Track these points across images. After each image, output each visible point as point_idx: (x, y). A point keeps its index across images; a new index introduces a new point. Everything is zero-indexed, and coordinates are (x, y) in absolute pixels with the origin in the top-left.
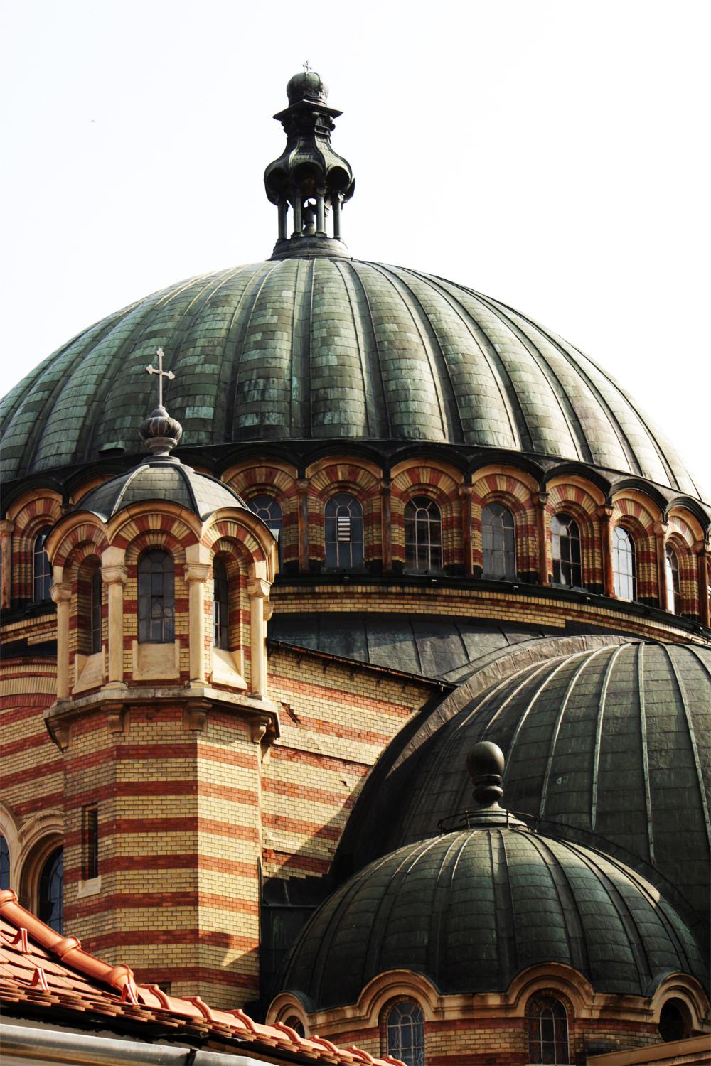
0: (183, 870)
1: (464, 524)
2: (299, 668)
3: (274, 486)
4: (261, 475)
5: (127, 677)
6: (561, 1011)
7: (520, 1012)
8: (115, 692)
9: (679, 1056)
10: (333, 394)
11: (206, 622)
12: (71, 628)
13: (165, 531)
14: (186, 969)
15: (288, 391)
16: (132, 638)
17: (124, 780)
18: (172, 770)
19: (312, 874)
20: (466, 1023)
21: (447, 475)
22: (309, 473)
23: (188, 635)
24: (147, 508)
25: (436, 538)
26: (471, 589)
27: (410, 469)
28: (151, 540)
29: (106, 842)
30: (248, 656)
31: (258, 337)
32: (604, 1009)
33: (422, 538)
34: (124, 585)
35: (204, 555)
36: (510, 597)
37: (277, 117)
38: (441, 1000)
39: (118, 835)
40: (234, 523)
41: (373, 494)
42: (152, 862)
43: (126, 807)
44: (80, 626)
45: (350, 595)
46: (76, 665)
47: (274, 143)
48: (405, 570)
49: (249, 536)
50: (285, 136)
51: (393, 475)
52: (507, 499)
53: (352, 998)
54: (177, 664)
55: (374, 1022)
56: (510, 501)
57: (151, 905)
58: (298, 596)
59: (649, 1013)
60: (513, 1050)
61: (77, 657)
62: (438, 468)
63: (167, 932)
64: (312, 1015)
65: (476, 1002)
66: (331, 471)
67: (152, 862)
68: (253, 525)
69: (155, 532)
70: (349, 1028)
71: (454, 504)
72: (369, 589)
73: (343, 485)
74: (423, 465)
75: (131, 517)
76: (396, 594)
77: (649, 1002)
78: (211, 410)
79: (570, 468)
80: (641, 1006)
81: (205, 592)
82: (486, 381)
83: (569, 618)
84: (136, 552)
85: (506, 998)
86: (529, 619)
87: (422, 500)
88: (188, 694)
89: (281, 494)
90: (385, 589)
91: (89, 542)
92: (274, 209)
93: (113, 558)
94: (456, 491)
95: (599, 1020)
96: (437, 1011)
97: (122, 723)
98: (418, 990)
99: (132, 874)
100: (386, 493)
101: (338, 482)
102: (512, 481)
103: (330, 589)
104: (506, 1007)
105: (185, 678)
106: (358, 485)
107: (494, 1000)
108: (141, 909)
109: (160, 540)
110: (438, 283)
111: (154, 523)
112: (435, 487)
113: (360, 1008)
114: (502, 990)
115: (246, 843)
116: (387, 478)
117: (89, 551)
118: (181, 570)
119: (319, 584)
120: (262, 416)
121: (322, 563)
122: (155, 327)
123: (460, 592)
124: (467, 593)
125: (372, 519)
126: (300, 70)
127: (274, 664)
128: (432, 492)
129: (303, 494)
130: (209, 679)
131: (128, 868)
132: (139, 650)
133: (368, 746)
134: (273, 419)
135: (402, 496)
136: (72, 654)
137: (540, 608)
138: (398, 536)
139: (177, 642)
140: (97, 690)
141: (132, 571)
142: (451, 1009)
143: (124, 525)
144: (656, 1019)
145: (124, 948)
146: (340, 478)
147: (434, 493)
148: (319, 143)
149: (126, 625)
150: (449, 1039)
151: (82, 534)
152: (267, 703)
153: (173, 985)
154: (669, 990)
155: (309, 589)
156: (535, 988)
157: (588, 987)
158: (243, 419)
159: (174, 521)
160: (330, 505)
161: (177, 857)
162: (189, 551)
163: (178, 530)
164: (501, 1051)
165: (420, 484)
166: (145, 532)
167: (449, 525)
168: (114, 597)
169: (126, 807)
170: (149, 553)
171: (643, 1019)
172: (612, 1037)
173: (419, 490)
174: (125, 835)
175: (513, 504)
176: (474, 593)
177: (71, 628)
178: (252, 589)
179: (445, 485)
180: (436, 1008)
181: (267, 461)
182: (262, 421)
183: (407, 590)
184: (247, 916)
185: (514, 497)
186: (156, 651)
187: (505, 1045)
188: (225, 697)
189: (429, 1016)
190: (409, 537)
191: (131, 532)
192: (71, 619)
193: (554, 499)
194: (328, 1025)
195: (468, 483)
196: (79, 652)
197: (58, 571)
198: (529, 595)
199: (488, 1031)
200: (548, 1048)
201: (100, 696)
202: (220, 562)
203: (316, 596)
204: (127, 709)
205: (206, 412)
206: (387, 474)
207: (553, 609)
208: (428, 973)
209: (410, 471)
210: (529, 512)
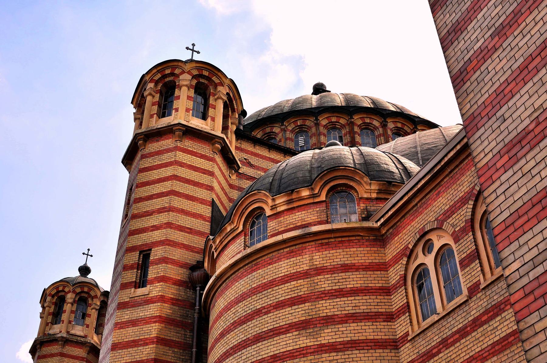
2: (255, 148)
4: (268, 130)
7: (323, 197)
14: (161, 241)
21: (343, 118)
24: (164, 66)
27: (327, 117)
32: (379, 192)
34: (153, 96)
38: (274, 200)
40: (207, 71)
52: (371, 126)
56: (372, 127)
60: (319, 220)
65: (294, 196)
68: (217, 72)
71: (347, 127)
73: (301, 127)
74: (333, 115)
75: (158, 71)
85: (312, 189)
95: (377, 199)
96: (273, 208)
101: (298, 126)
102: (372, 119)
106: (306, 126)
107: (305, 193)
112: (338, 122)
127: (241, 143)
128: (338, 125)
142: (281, 205)
145: (131, 237)
146: (299, 124)
147: (339, 125)
156: (332, 184)
164: (311, 221)
173: (332, 125)
175: (374, 128)
179: (342, 121)
180: (271, 207)
185: (373, 125)
187: (314, 218)
199: (303, 212)
210: (381, 129)
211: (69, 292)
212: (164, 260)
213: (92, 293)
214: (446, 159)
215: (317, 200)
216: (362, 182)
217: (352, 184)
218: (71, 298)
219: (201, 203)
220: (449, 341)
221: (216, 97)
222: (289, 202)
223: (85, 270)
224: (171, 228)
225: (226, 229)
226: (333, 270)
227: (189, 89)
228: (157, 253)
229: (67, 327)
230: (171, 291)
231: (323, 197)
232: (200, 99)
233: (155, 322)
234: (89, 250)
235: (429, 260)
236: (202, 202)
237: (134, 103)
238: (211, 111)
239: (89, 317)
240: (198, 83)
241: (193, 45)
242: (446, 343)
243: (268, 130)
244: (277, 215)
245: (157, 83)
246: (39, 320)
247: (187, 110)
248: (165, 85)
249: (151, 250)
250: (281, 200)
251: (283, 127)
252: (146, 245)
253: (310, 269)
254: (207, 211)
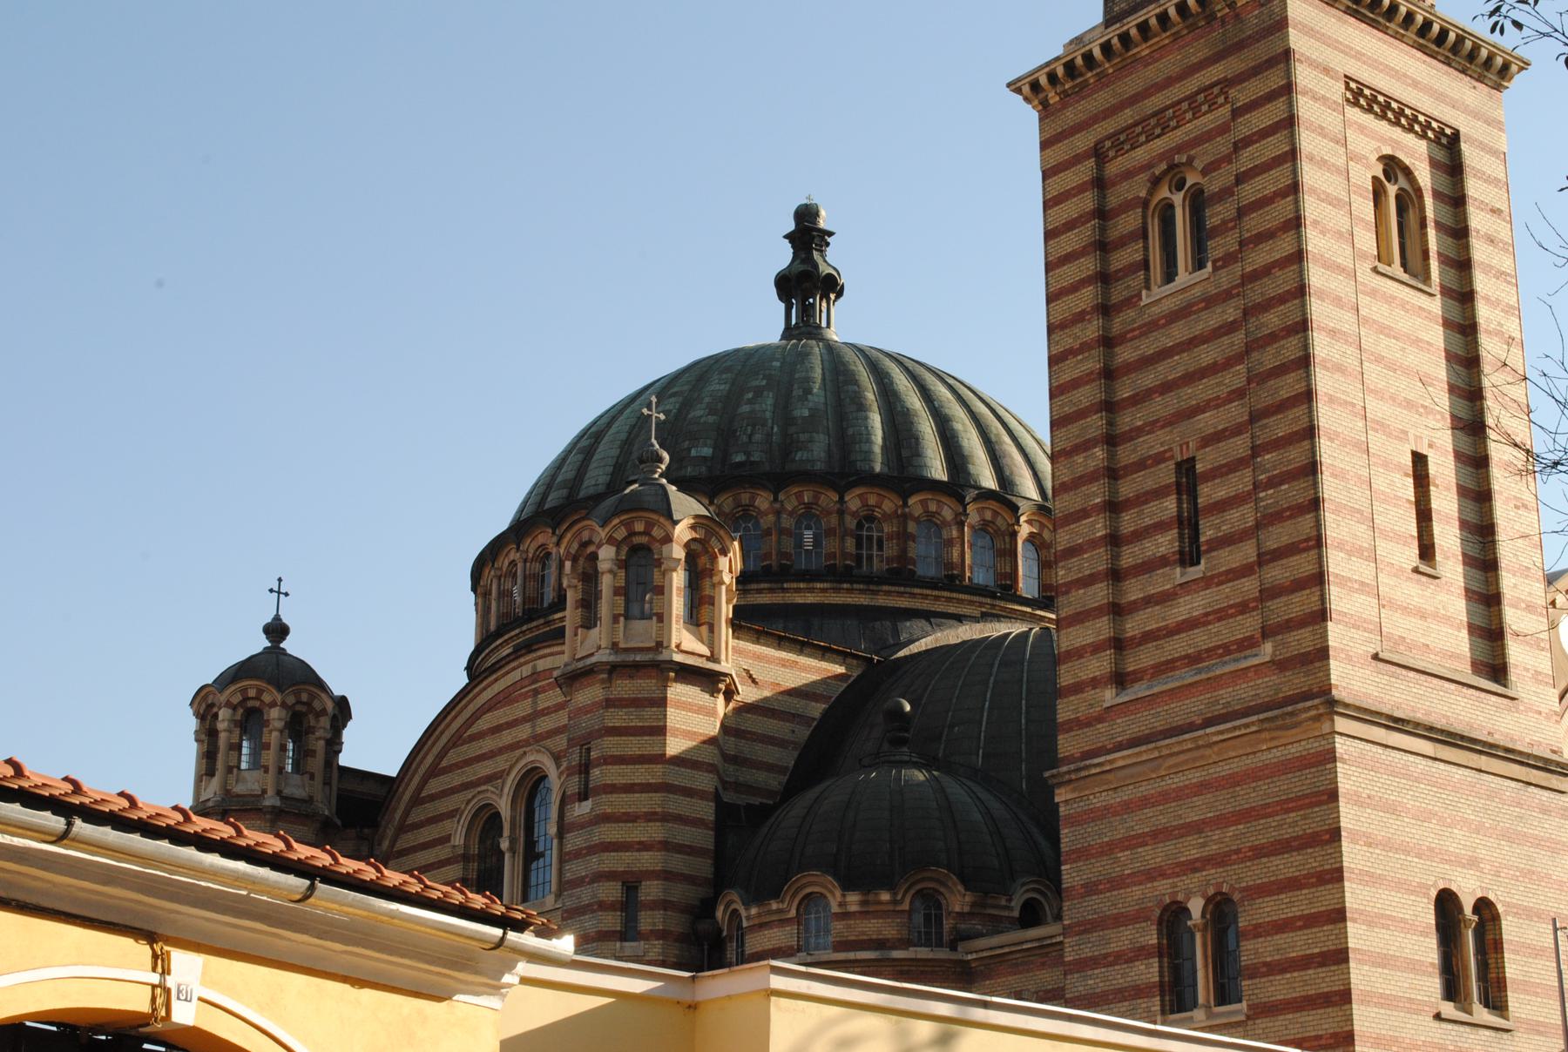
0: (654, 794)
1: (904, 537)
3: (755, 507)
4: (745, 498)
5: (614, 646)
6: (939, 906)
7: (906, 906)
8: (604, 656)
9: (1027, 942)
10: (803, 437)
11: (678, 605)
12: (577, 608)
13: (647, 533)
14: (653, 872)
15: (770, 435)
16: (620, 615)
17: (610, 725)
18: (647, 717)
19: (765, 801)
20: (864, 914)
22: (781, 497)
23: (663, 613)
25: (880, 548)
26: (905, 586)
27: (861, 494)
28: (637, 540)
29: (595, 772)
30: (711, 629)
31: (750, 395)
32: (973, 905)
33: (870, 548)
34: (615, 575)
35: (678, 552)
36: (936, 593)
37: (786, 237)
38: (844, 896)
39: (604, 767)
41: (831, 513)
42: (630, 788)
43: (611, 745)
44: (583, 606)
45: (811, 590)
46: (579, 637)
47: (784, 256)
48: (855, 572)
49: (714, 538)
50: (792, 251)
51: (846, 499)
53: (776, 894)
54: (654, 635)
55: (793, 913)
57: (626, 821)
58: (771, 590)
59: (1010, 909)
61: (580, 630)
62: (882, 493)
63: (640, 843)
64: (747, 905)
65: (871, 897)
66: (799, 495)
67: (630, 788)
68: (717, 529)
69: (640, 533)
70: (775, 917)
72: (826, 585)
73: (808, 506)
75: (621, 522)
76: (847, 589)
77: (1010, 900)
78: (711, 450)
79: (987, 495)
80: (1003, 902)
81: (678, 579)
82: (927, 428)
83: (984, 610)
84: (625, 549)
85: (895, 894)
86: (952, 610)
87: (870, 518)
88: (661, 658)
89: (760, 513)
90: (839, 586)
91: (590, 542)
92: (782, 306)
93: (606, 554)
94: (896, 511)
95: (968, 913)
96: (841, 905)
97: (610, 680)
98: (826, 888)
99: (613, 797)
100: (841, 513)
103: (795, 585)
104: (894, 902)
105: (660, 646)
107: (885, 896)
108: (620, 824)
109: (644, 540)
110: (897, 359)
111: (639, 527)
112: (880, 508)
113: (782, 902)
114: (892, 888)
115: (705, 774)
117: (591, 549)
118: (659, 563)
119: (787, 581)
120: (748, 454)
121: (791, 566)
122: (675, 390)
123: (897, 589)
124: (902, 589)
125: (830, 532)
126: (805, 201)
129: (778, 513)
130: (678, 646)
131: (611, 793)
132: (625, 627)
133: (813, 704)
134: (756, 457)
135: (854, 514)
136: (577, 628)
137: (960, 601)
138: (850, 544)
139: (655, 618)
140: (592, 655)
141: (623, 564)
143: (615, 528)
144: (1016, 914)
145: (606, 854)
146: (806, 501)
148: (816, 255)
149: (613, 605)
150: (849, 927)
151: (585, 535)
152: (725, 666)
153: (643, 883)
154: (1027, 891)
155: (779, 585)
156: (918, 887)
157: (960, 888)
158: (733, 457)
159: (654, 525)
160: (798, 524)
161: (650, 784)
162: (665, 548)
163: (657, 532)
164: (890, 936)
165: (867, 505)
166: (632, 534)
167: (890, 537)
168: (606, 583)
169: (611, 745)
170: (635, 549)
171: (1006, 913)
172: (980, 927)
174: (609, 767)
176: (908, 590)
177: (577, 608)
178: (716, 579)
181: (752, 487)
182: (748, 457)
183: (855, 586)
184: (705, 831)
186: (639, 626)
188: (690, 661)
189: (835, 909)
190: (859, 545)
191: (621, 534)
192: (577, 601)
193: (973, 517)
194: (759, 915)
195: (905, 504)
196: (582, 626)
197: (568, 564)
198: (952, 591)
199: (881, 921)
200: (928, 934)
201: (593, 659)
202: (691, 558)
203: (784, 590)
204: (614, 669)
205: (707, 451)
206: (841, 498)
207: (971, 603)
208: (836, 876)
209: (860, 496)
211: (273, 704)
212: (665, 905)
213: (317, 705)
215: (899, 908)
217: (942, 890)
218: (280, 719)
223: (277, 630)
228: (651, 890)
229: (278, 783)
234: (280, 580)
239: (312, 756)
243: (745, 498)
244: (845, 915)
246: (195, 745)
250: (853, 898)
254: (707, 810)
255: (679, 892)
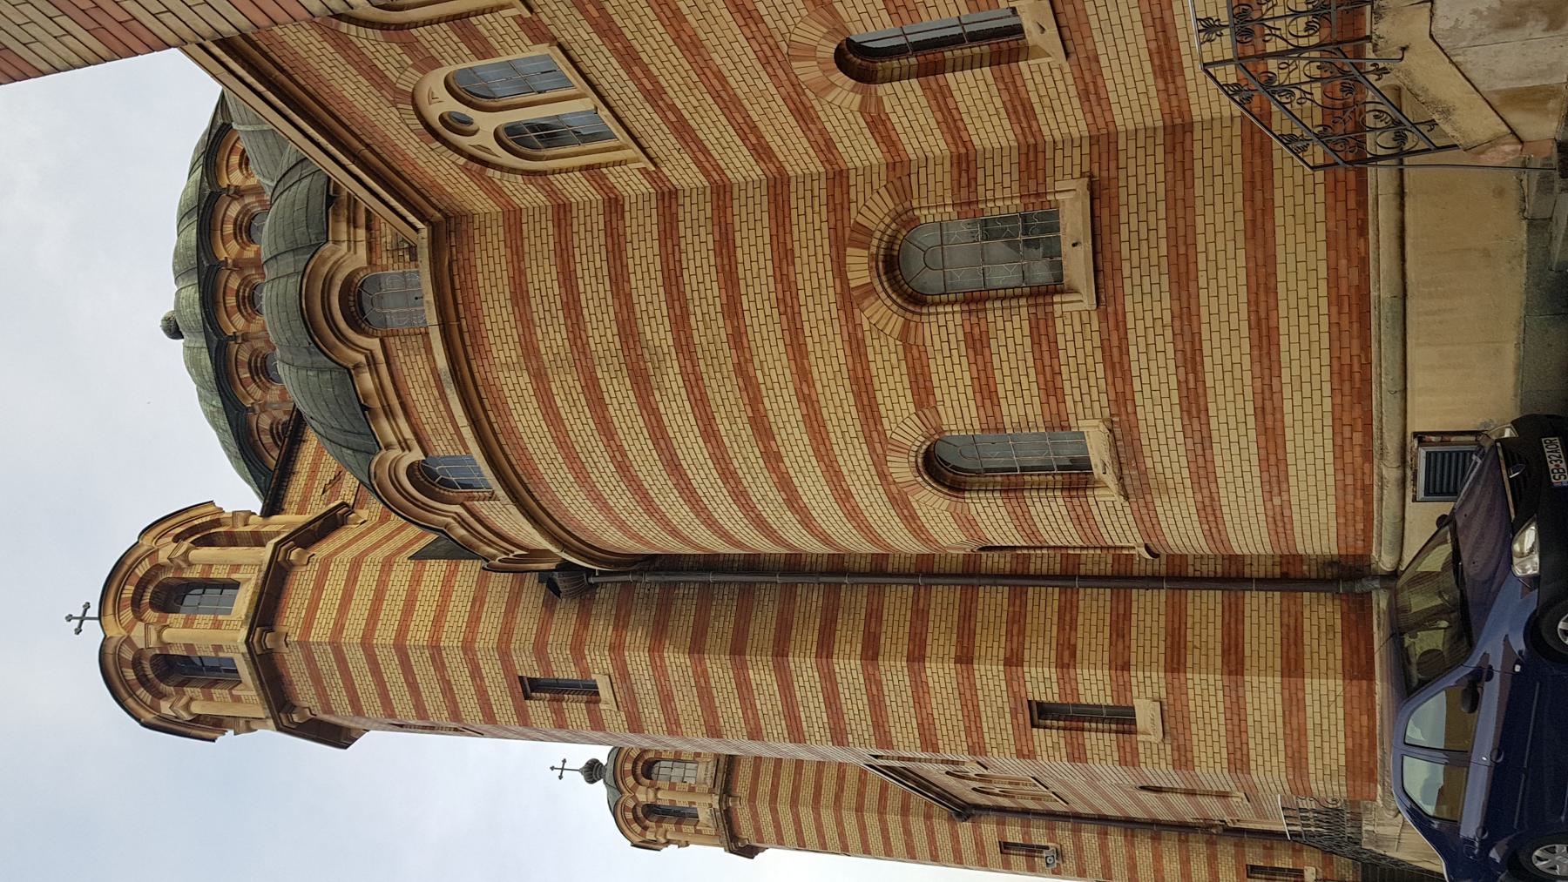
7: (374, 344)
16: (232, 695)
32: (352, 222)
34: (192, 699)
38: (388, 447)
60: (423, 351)
68: (125, 568)
71: (247, 273)
75: (131, 696)
85: (357, 366)
101: (252, 377)
106: (250, 360)
107: (367, 381)
116: (234, 337)
127: (291, 503)
142: (397, 431)
156: (343, 325)
180: (403, 450)
185: (238, 216)
187: (420, 362)
210: (247, 200)
212: (540, 650)
214: (250, 79)
215: (380, 356)
216: (334, 259)
219: (419, 582)
220: (649, 87)
221: (184, 565)
222: (389, 413)
224: (474, 640)
225: (461, 538)
226: (526, 322)
227: (168, 626)
228: (528, 667)
230: (601, 629)
231: (374, 344)
232: (189, 600)
233: (662, 659)
235: (487, 124)
236: (416, 580)
237: (211, 735)
238: (219, 573)
240: (154, 605)
241: (69, 618)
242: (653, 93)
243: (267, 439)
245: (160, 695)
247: (217, 625)
248: (163, 677)
249: (521, 678)
251: (257, 408)
252: (510, 687)
253: (527, 369)
254: (436, 569)
255: (526, 623)
